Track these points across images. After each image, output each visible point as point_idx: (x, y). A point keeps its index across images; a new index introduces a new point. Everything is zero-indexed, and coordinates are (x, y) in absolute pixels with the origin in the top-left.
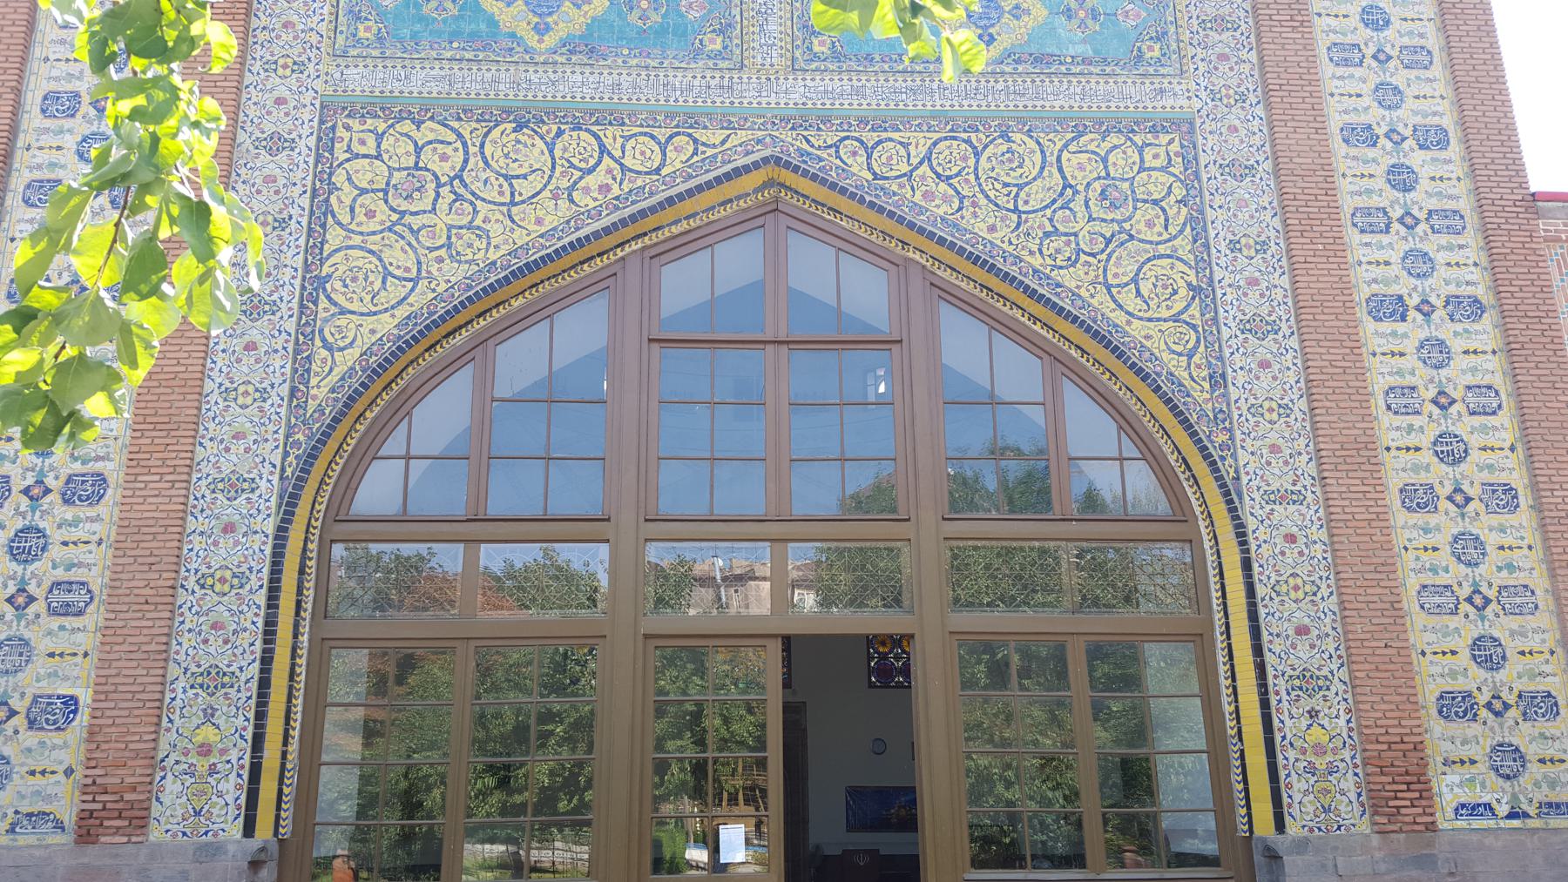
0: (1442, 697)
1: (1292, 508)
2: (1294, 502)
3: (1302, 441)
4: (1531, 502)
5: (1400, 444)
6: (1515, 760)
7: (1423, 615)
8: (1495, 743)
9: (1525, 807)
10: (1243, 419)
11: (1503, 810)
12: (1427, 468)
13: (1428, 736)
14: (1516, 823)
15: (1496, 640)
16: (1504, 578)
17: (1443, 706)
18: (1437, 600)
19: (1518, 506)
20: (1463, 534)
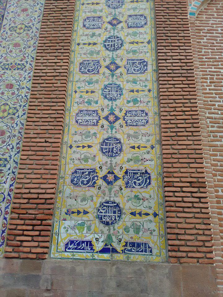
0: (76, 172)
1: (16, 71)
2: (18, 69)
3: (32, 42)
4: (154, 68)
5: (86, 42)
6: (115, 212)
7: (76, 126)
8: (104, 201)
9: (115, 245)
10: (5, 33)
11: (99, 246)
12: (98, 53)
13: (60, 195)
14: (106, 256)
15: (117, 140)
16: (131, 106)
17: (74, 178)
18: (87, 118)
19: (146, 70)
20: (111, 85)
